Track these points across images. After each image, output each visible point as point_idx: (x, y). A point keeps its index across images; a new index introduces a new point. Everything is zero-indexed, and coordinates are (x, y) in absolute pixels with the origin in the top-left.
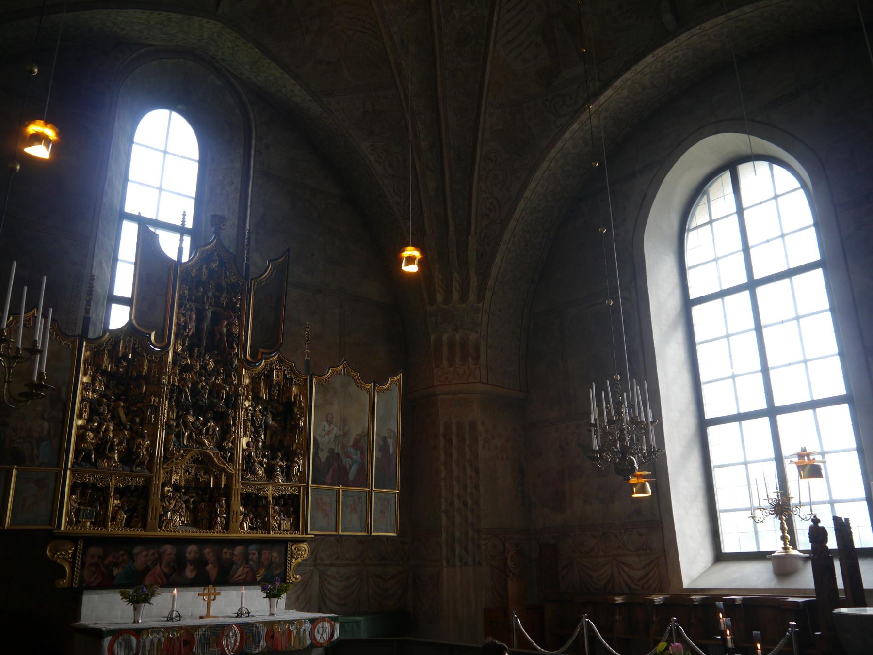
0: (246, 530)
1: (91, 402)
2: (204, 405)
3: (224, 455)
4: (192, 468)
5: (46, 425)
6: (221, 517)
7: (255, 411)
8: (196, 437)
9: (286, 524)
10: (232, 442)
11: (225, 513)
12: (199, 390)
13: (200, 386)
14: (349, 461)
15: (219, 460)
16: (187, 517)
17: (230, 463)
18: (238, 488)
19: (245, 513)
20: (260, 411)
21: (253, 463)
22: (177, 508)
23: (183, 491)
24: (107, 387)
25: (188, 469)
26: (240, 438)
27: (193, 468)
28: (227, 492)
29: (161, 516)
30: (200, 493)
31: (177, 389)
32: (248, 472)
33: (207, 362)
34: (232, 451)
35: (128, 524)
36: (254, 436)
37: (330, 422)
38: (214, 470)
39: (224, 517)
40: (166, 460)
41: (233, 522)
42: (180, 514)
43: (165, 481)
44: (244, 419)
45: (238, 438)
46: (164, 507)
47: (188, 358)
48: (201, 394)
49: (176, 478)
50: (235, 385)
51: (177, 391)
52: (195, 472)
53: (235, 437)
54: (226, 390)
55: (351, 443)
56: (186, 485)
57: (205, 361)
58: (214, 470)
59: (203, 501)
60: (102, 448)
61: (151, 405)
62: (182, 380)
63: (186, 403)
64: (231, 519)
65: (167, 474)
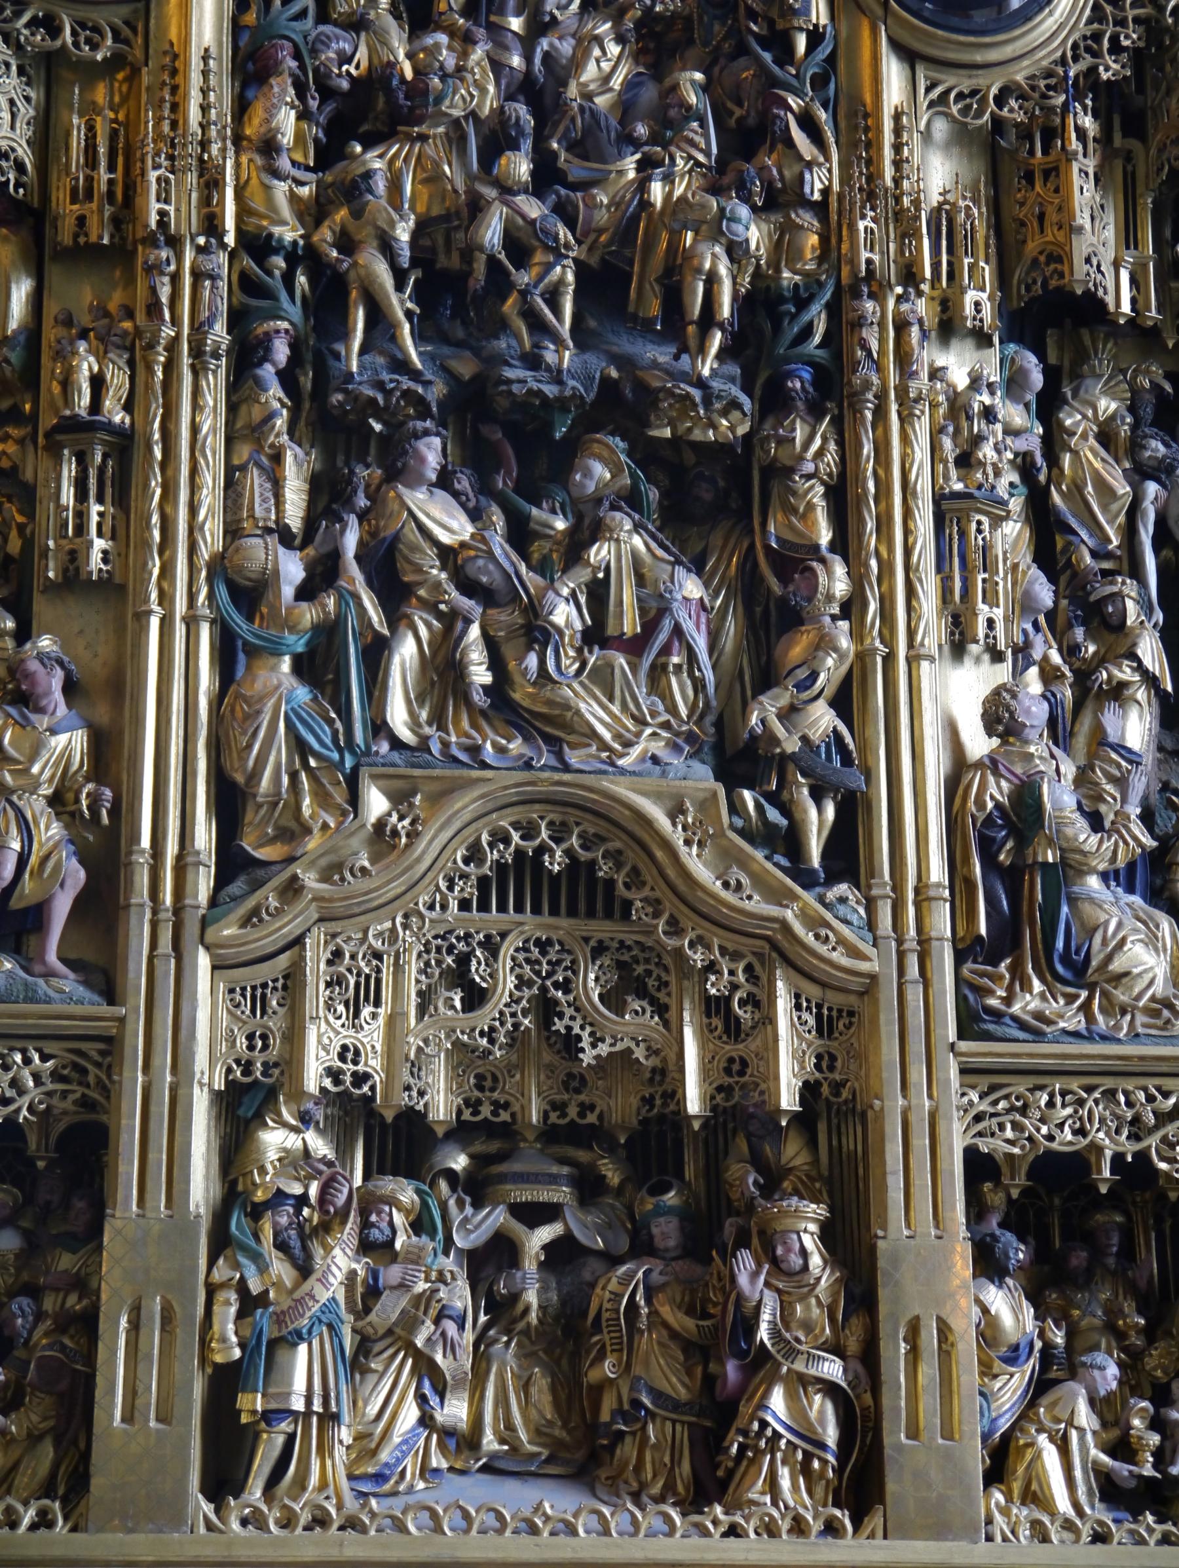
0: (1063, 1504)
2: (550, 390)
3: (773, 815)
4: (491, 947)
6: (801, 1383)
7: (1054, 441)
8: (496, 663)
10: (842, 702)
11: (837, 1349)
12: (492, 261)
13: (492, 233)
15: (727, 858)
16: (502, 1400)
17: (842, 889)
19: (1048, 1347)
20: (1106, 437)
22: (389, 1309)
23: (460, 1162)
25: (464, 960)
26: (913, 660)
27: (507, 950)
30: (613, 1176)
31: (302, 280)
32: (1017, 971)
33: (566, 48)
36: (1070, 651)
38: (698, 958)
39: (830, 1389)
40: (236, 887)
41: (913, 1434)
42: (425, 1367)
43: (247, 1068)
44: (939, 499)
45: (889, 660)
46: (249, 1303)
47: (391, 23)
48: (510, 306)
49: (348, 1037)
50: (821, 208)
52: (522, 983)
53: (863, 658)
54: (736, 251)
56: (473, 1104)
57: (544, 44)
58: (698, 958)
59: (642, 1247)
61: (73, 425)
63: (380, 386)
64: (895, 1399)
65: (260, 1003)
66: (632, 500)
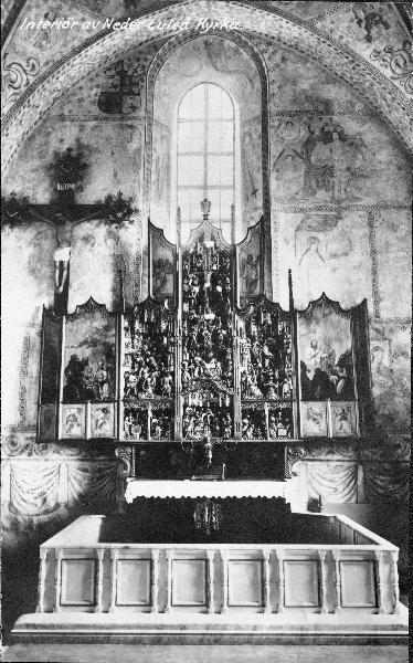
1: (132, 355)
5: (105, 373)
9: (283, 432)
14: (335, 377)
18: (238, 406)
21: (250, 385)
24: (144, 343)
28: (231, 409)
29: (184, 429)
34: (232, 378)
35: (163, 435)
37: (314, 347)
51: (187, 340)
55: (336, 362)
60: (141, 386)
62: (191, 330)
66: (214, 357)
